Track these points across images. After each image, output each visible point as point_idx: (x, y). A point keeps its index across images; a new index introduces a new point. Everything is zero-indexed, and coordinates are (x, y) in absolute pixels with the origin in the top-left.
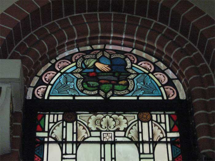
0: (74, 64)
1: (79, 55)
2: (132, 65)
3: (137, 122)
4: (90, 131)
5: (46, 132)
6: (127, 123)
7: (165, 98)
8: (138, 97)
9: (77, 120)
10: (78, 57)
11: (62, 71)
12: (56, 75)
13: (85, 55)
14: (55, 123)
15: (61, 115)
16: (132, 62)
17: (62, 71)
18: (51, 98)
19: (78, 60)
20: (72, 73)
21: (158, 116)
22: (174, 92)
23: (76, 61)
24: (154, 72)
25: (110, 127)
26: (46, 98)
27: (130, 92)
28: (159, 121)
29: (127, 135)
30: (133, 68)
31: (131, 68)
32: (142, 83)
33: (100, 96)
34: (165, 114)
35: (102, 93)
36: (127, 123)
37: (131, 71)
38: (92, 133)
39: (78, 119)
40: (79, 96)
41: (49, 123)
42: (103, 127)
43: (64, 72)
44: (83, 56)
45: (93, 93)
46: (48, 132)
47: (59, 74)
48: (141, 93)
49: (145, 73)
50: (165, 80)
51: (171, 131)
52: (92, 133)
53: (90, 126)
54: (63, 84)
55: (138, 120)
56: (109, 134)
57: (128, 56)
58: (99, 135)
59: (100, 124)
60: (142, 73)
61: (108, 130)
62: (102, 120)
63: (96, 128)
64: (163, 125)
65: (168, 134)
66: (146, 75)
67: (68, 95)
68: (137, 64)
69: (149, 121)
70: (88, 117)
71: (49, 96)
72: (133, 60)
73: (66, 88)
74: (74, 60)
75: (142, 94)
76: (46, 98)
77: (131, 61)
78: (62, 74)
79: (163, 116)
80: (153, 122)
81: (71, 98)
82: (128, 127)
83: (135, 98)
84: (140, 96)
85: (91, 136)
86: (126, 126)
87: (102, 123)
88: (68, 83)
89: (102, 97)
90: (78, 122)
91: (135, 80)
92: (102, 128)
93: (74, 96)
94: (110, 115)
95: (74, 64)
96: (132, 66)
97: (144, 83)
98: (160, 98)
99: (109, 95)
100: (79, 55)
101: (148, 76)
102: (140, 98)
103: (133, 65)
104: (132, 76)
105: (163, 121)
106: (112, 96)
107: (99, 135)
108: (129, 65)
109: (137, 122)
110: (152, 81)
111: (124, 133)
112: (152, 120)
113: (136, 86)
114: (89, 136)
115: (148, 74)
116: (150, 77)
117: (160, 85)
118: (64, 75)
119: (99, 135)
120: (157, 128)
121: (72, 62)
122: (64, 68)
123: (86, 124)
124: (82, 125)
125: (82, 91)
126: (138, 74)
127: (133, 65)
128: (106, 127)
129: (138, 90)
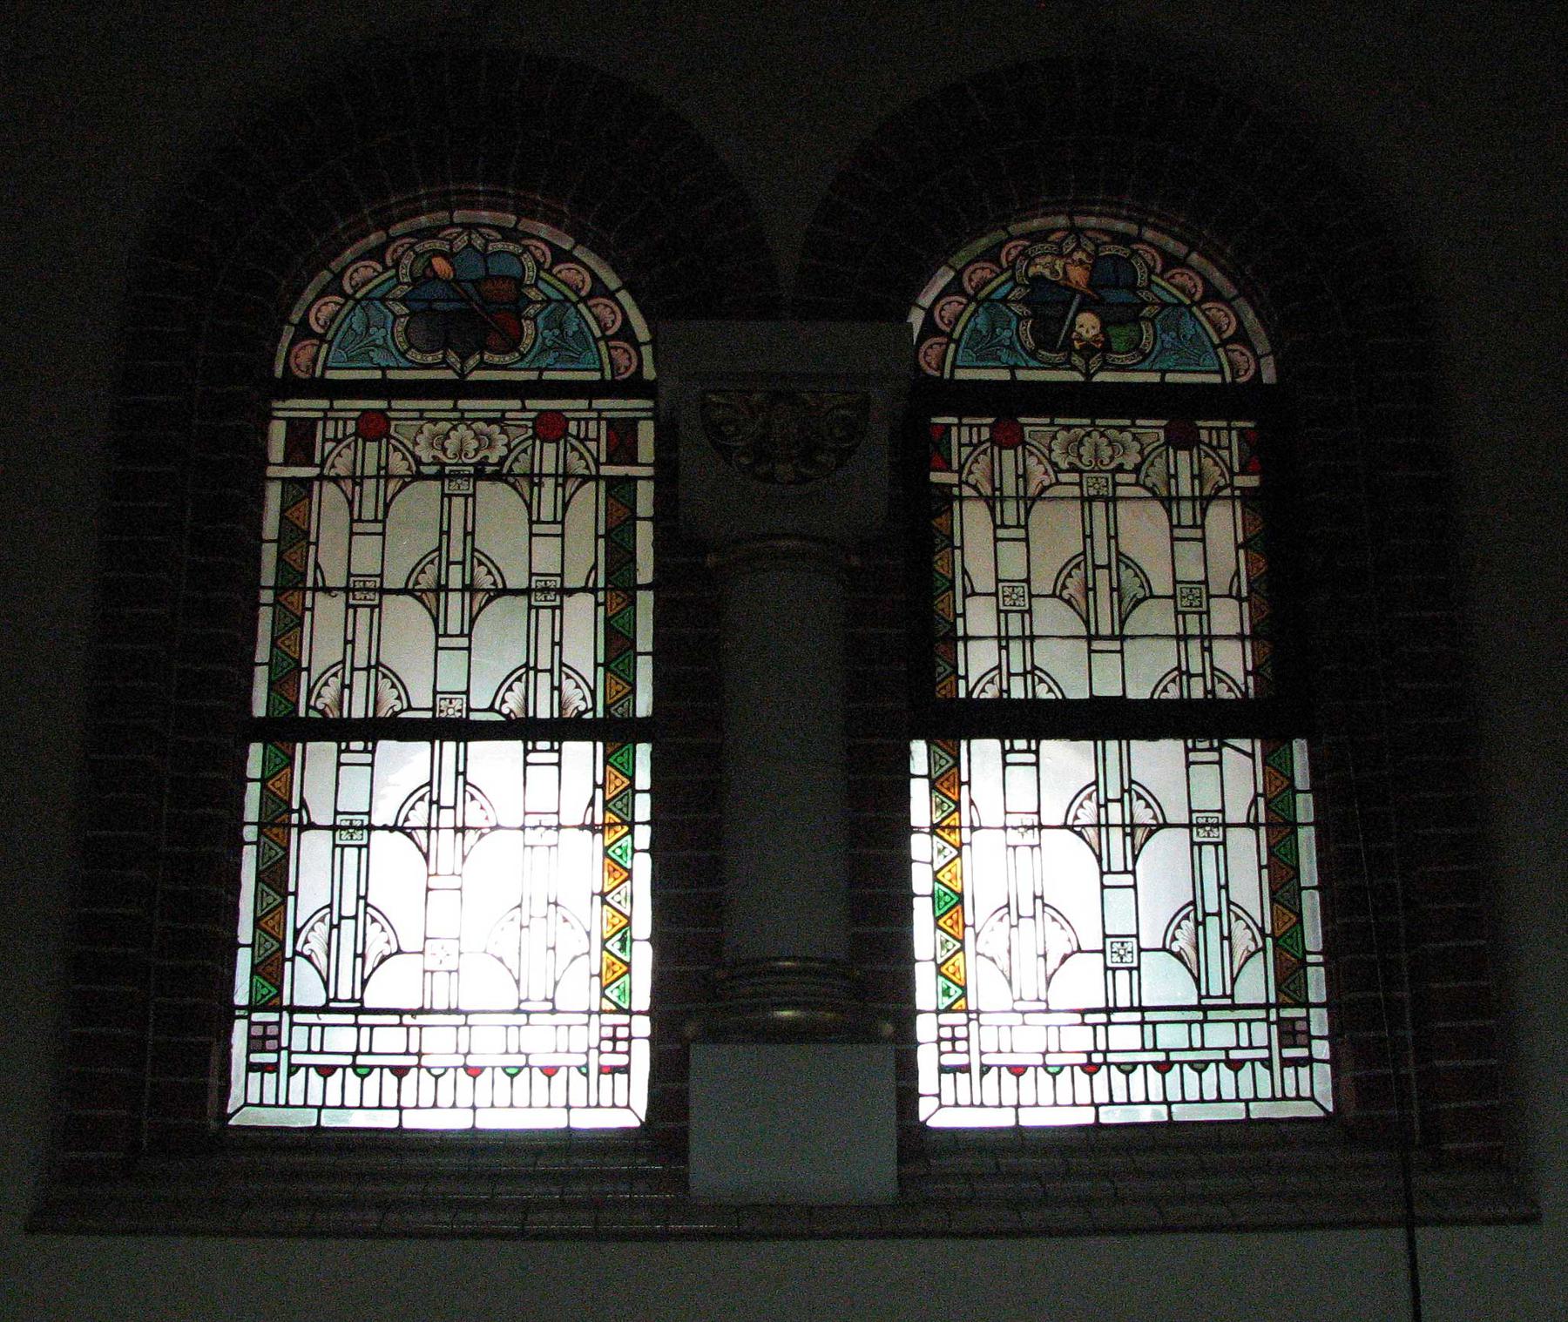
0: (392, 272)
1: (402, 246)
2: (538, 275)
3: (530, 442)
4: (418, 462)
6: (508, 445)
7: (608, 376)
8: (541, 370)
9: (389, 437)
10: (400, 250)
11: (358, 295)
12: (343, 306)
13: (417, 243)
15: (353, 422)
16: (539, 266)
17: (358, 295)
18: (330, 375)
19: (400, 258)
20: (383, 300)
22: (630, 359)
23: (397, 264)
24: (591, 295)
25: (466, 455)
26: (318, 373)
27: (523, 356)
30: (541, 285)
31: (535, 285)
32: (557, 332)
33: (449, 367)
34: (599, 419)
35: (453, 358)
36: (508, 445)
37: (533, 294)
39: (392, 431)
40: (399, 368)
41: (325, 440)
43: (365, 297)
44: (412, 246)
45: (430, 359)
46: (322, 465)
47: (351, 303)
48: (549, 359)
49: (567, 299)
50: (613, 322)
51: (610, 462)
53: (418, 451)
54: (359, 331)
55: (533, 438)
57: (533, 248)
59: (443, 445)
60: (557, 301)
61: (460, 462)
62: (447, 436)
63: (434, 457)
64: (592, 445)
65: (602, 468)
66: (568, 305)
67: (370, 365)
68: (549, 271)
70: (416, 429)
71: (325, 368)
72: (542, 260)
73: (365, 346)
74: (389, 262)
75: (550, 360)
76: (318, 373)
77: (537, 261)
78: (358, 301)
79: (593, 425)
81: (378, 375)
82: (510, 451)
83: (533, 376)
84: (547, 369)
86: (504, 451)
87: (447, 444)
88: (372, 331)
89: (455, 371)
90: (393, 441)
91: (540, 320)
92: (446, 456)
93: (383, 369)
95: (392, 272)
96: (538, 278)
97: (562, 331)
98: (596, 376)
99: (472, 362)
100: (402, 246)
101: (573, 309)
102: (547, 375)
103: (543, 274)
104: (531, 311)
105: (592, 435)
106: (477, 368)
108: (530, 275)
109: (530, 442)
110: (583, 325)
112: (566, 434)
113: (540, 340)
115: (575, 305)
116: (578, 311)
117: (598, 333)
118: (364, 303)
120: (576, 454)
121: (386, 269)
122: (364, 284)
123: (410, 446)
124: (400, 451)
125: (403, 354)
126: (549, 300)
127: (543, 274)
129: (544, 350)
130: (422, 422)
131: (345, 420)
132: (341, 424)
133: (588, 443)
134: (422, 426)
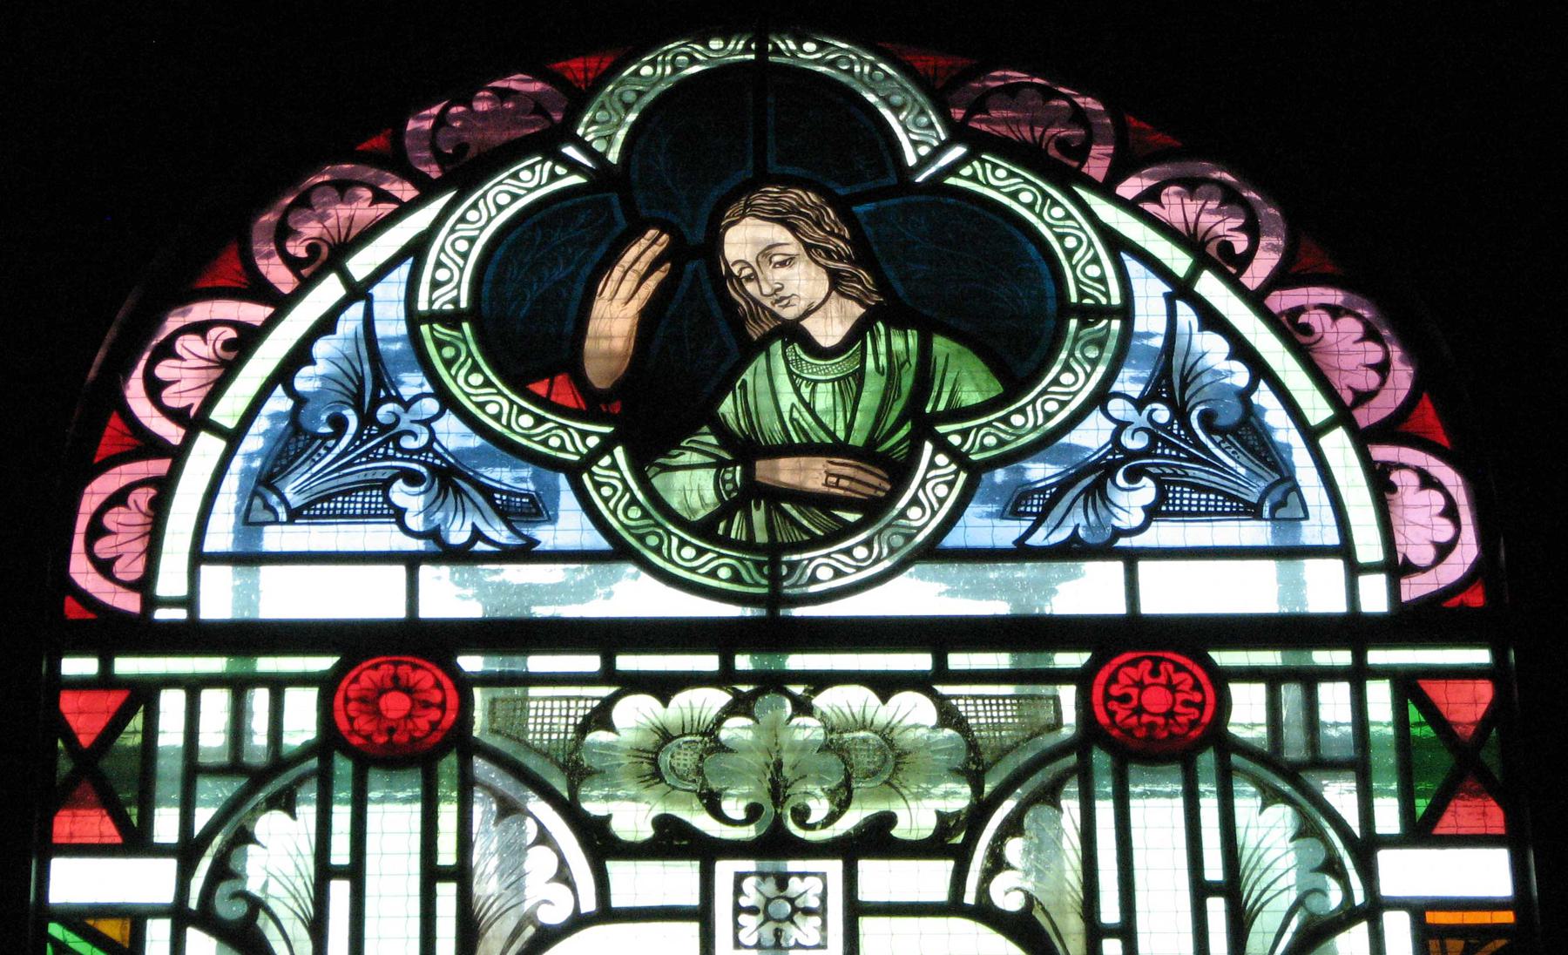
5: (162, 851)
14: (258, 777)
21: (1291, 694)
28: (1295, 746)
29: (970, 898)
38: (614, 868)
42: (734, 807)
52: (614, 868)
56: (802, 875)
58: (692, 899)
69: (1200, 746)
80: (1235, 759)
85: (607, 913)
94: (798, 690)
107: (690, 896)
111: (943, 869)
114: (589, 904)
119: (690, 896)
123: (560, 785)
128: (754, 813)
130: (606, 691)
131: (278, 685)
132: (260, 699)
133: (1312, 778)
134: (608, 704)
